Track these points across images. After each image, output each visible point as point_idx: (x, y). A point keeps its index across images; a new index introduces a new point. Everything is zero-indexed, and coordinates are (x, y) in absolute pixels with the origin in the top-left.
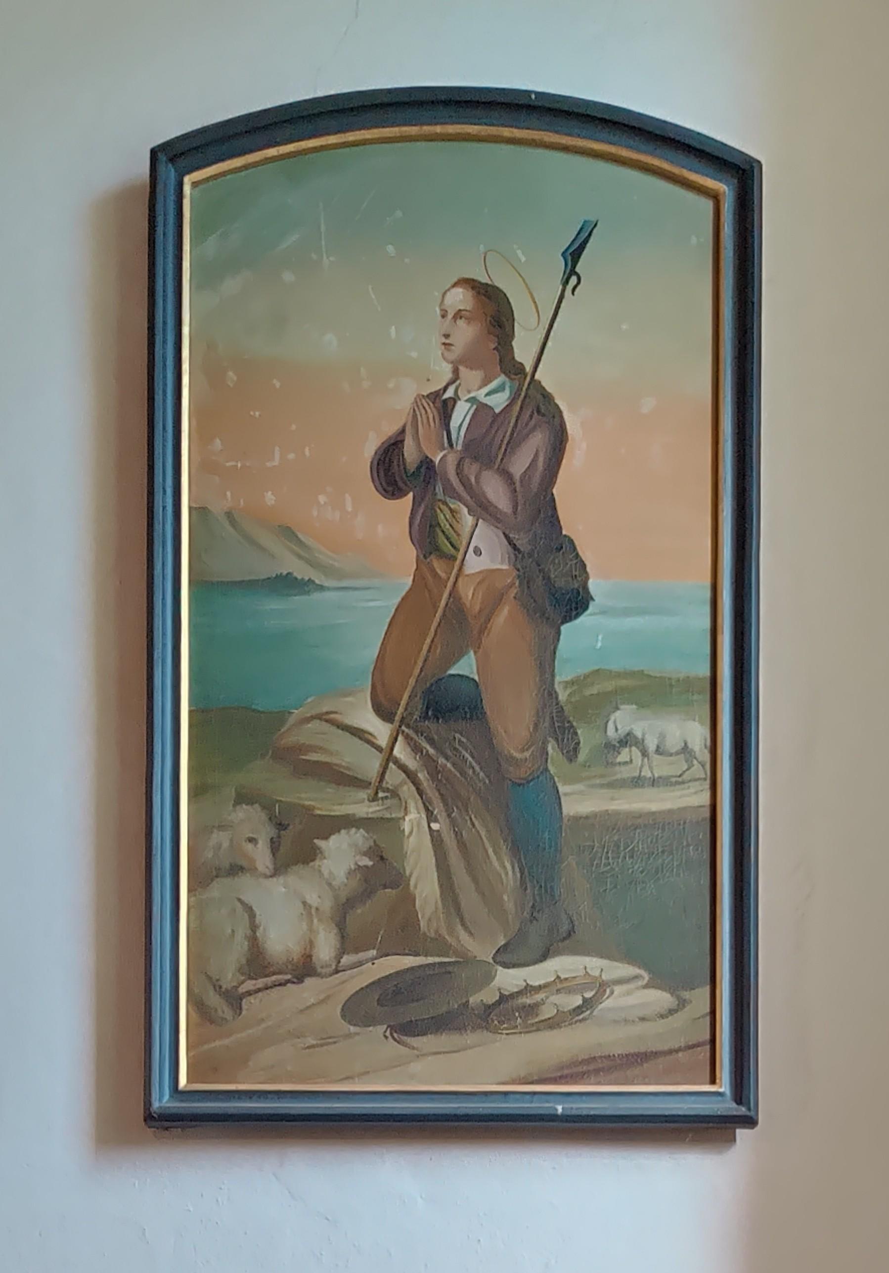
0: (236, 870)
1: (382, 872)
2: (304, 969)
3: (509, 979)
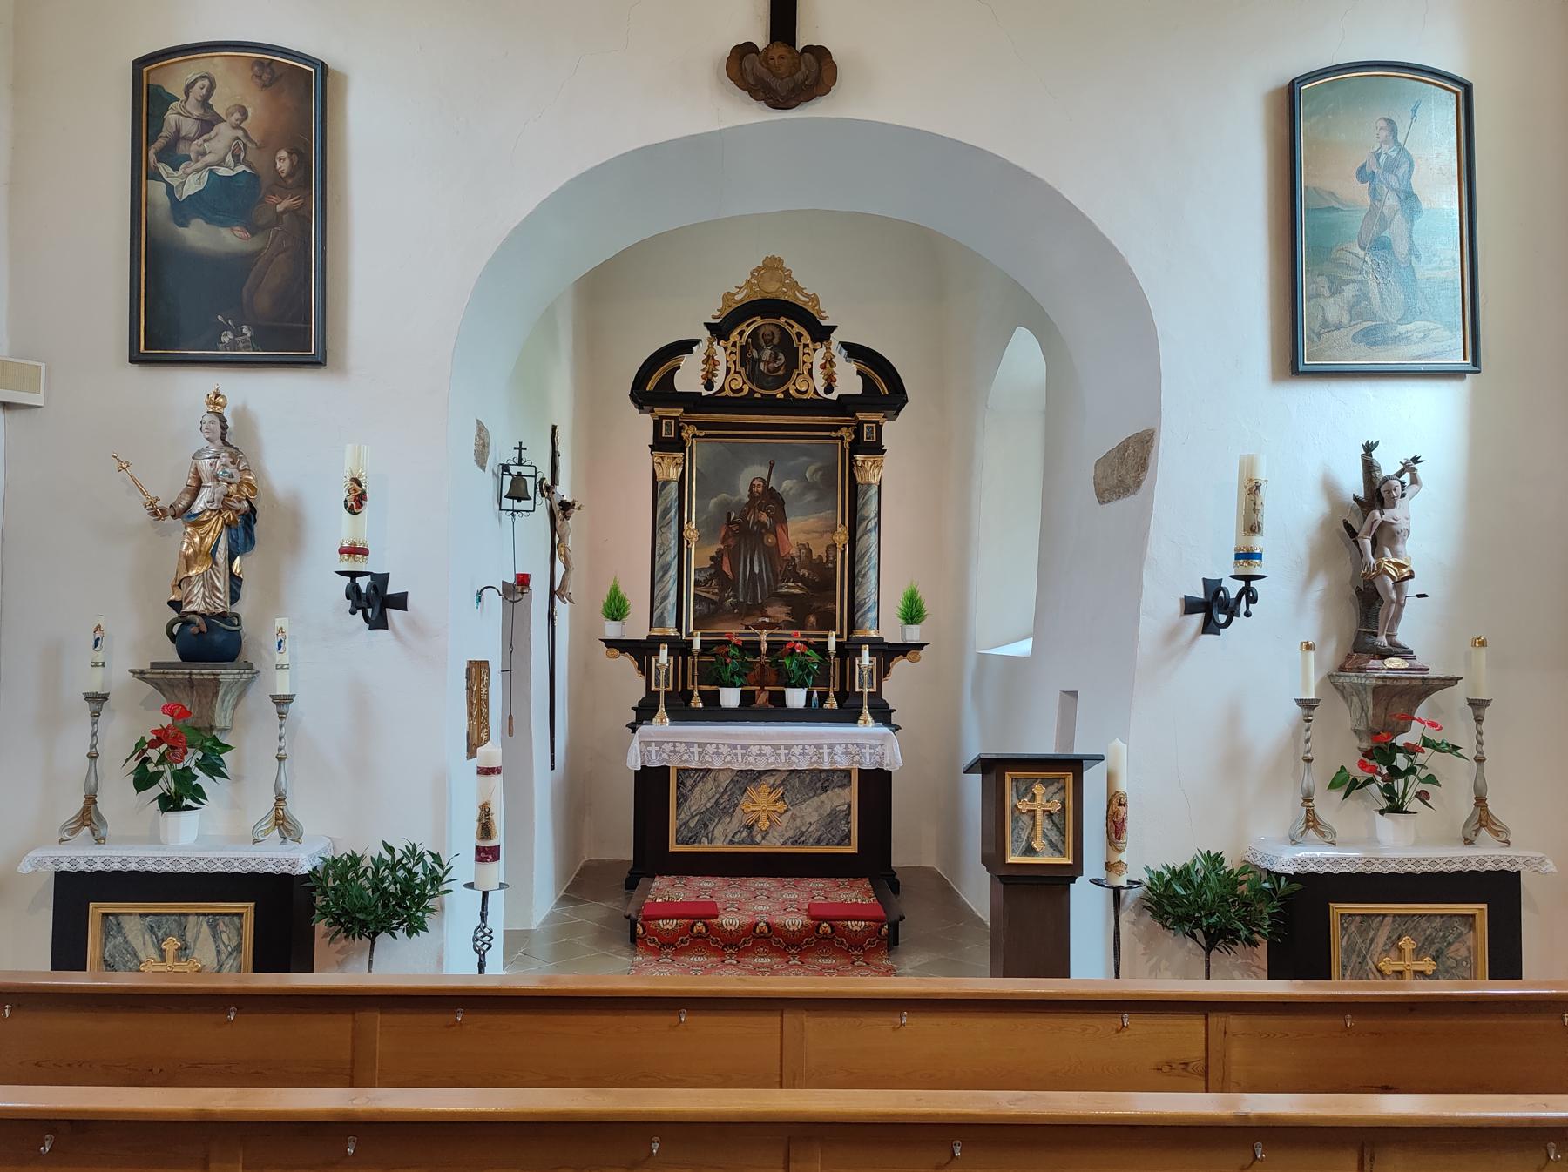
0: (1318, 296)
1: (1364, 296)
2: (1339, 327)
3: (1401, 329)
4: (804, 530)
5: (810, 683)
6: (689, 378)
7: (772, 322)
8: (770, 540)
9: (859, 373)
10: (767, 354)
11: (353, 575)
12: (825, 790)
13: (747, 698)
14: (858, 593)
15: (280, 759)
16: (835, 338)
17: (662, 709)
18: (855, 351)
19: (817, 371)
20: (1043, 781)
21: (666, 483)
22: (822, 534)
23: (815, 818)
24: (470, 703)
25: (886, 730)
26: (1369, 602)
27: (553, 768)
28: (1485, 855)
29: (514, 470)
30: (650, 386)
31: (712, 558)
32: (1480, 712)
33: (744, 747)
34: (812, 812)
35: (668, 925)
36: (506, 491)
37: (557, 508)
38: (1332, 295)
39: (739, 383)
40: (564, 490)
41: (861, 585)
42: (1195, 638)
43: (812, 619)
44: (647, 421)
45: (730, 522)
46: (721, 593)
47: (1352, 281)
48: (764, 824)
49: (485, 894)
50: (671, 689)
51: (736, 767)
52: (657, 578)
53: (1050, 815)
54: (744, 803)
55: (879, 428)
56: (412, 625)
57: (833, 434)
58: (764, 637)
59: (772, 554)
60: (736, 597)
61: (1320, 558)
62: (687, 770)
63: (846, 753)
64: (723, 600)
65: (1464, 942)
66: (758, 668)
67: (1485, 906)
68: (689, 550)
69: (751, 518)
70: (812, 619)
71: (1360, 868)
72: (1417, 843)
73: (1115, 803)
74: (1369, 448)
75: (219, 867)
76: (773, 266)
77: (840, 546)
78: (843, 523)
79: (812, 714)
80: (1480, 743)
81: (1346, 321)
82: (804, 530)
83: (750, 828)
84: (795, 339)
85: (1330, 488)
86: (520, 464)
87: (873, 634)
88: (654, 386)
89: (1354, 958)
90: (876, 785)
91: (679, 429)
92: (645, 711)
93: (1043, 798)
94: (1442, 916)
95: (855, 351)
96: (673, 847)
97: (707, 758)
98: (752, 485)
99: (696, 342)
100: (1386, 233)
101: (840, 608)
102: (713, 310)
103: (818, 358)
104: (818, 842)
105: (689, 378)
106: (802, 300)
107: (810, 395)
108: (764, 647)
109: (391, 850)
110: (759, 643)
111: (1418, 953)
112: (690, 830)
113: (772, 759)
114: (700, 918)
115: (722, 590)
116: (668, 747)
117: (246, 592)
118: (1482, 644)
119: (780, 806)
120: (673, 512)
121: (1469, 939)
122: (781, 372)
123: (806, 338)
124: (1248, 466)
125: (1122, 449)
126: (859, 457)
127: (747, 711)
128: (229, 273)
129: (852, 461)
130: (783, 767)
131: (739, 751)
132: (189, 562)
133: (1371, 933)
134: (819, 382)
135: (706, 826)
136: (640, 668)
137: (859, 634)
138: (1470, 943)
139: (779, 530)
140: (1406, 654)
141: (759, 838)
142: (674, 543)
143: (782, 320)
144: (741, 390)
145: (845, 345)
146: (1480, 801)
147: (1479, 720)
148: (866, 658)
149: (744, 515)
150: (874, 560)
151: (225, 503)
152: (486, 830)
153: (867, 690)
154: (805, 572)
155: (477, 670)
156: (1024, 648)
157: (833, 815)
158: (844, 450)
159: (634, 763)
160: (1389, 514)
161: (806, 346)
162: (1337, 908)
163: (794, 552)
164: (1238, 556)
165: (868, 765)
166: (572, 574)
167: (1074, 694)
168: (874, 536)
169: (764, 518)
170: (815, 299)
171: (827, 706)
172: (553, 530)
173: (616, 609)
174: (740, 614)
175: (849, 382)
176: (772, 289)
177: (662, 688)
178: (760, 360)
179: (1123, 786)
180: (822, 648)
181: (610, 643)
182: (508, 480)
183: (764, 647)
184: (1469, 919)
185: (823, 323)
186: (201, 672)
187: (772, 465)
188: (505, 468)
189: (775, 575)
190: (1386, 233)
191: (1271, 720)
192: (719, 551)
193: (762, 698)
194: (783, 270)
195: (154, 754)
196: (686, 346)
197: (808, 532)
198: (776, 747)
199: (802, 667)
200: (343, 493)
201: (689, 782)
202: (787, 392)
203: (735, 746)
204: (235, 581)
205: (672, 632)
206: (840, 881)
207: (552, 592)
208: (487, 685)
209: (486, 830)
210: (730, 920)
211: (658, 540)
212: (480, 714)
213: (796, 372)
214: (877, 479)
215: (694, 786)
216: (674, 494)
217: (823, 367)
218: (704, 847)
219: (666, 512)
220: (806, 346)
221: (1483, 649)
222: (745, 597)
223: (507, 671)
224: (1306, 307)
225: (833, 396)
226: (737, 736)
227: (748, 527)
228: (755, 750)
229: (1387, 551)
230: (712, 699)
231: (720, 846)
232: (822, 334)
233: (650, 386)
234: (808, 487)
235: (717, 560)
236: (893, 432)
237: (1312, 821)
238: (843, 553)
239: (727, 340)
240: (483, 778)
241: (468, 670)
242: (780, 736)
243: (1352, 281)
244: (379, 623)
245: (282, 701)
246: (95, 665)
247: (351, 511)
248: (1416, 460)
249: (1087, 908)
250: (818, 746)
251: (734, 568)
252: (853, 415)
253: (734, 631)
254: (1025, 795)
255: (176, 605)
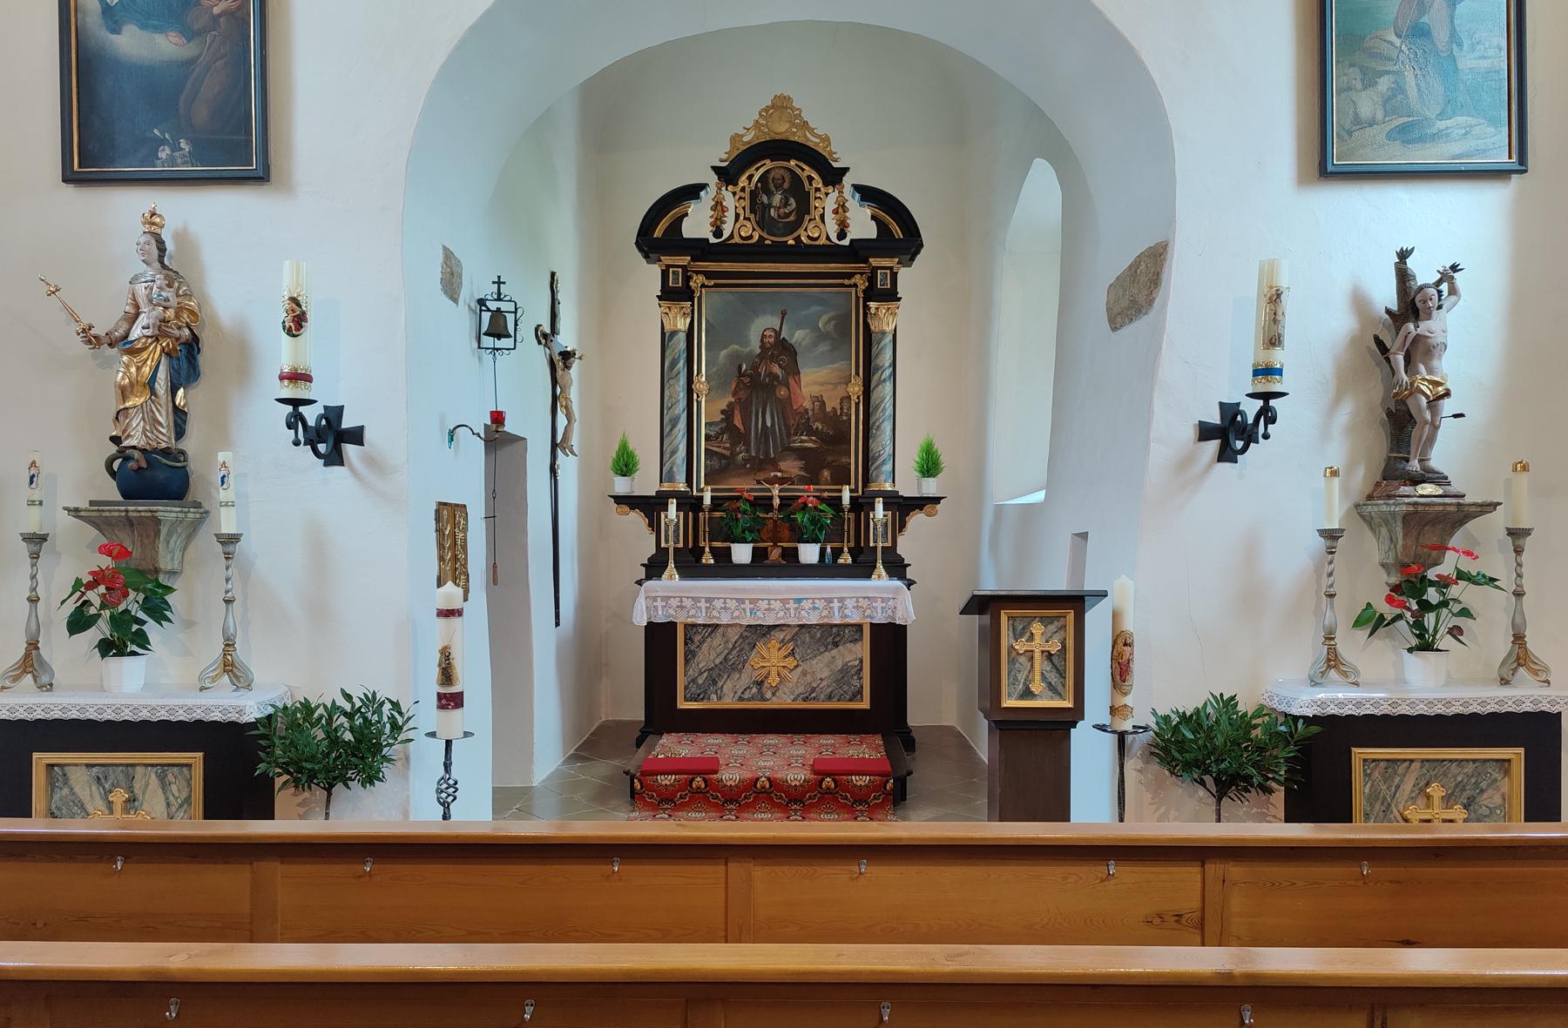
0: (1349, 89)
1: (1398, 89)
2: (1372, 123)
3: (1441, 125)
4: (818, 381)
5: (822, 538)
6: (697, 223)
7: (781, 163)
8: (783, 392)
9: (873, 218)
10: (777, 199)
11: (296, 403)
12: (836, 645)
13: (759, 555)
14: (873, 445)
15: (228, 602)
16: (848, 180)
17: (671, 565)
18: (868, 194)
19: (829, 216)
20: (1042, 619)
21: (674, 333)
22: (836, 385)
23: (826, 673)
24: (441, 546)
25: (898, 583)
26: (1402, 424)
27: (557, 624)
28: (1523, 696)
29: (493, 306)
30: (658, 233)
31: (723, 412)
32: (1520, 542)
33: (752, 601)
34: (822, 666)
35: (666, 780)
36: (485, 328)
37: (557, 358)
38: (1365, 88)
39: (749, 231)
40: (567, 338)
41: (875, 436)
42: (1210, 466)
43: (826, 473)
44: (655, 271)
45: (741, 375)
46: (733, 445)
47: (1388, 72)
48: (774, 680)
49: (448, 743)
50: (681, 545)
51: (745, 623)
52: (666, 430)
53: (1049, 656)
54: (754, 659)
55: (894, 276)
56: (372, 462)
57: (846, 282)
58: (776, 492)
59: (784, 407)
60: (748, 451)
61: (1346, 379)
62: (694, 626)
63: (857, 607)
64: (734, 455)
65: (1498, 789)
66: (770, 524)
67: (1521, 750)
68: (699, 403)
69: (762, 370)
70: (826, 473)
71: (1385, 709)
72: (1449, 683)
73: (1121, 645)
74: (1403, 255)
75: (163, 715)
76: (781, 105)
77: (854, 398)
78: (857, 373)
79: (825, 569)
80: (1519, 576)
81: (1380, 116)
82: (818, 381)
83: (760, 684)
84: (806, 183)
85: (1359, 303)
86: (499, 299)
87: (888, 487)
88: (658, 235)
89: (1378, 805)
90: (889, 642)
91: (687, 279)
92: (654, 568)
93: (1041, 637)
94: (1474, 761)
95: (868, 194)
96: (682, 705)
97: (715, 613)
98: (763, 336)
99: (703, 187)
100: (1425, 19)
101: (854, 462)
102: (720, 153)
103: (830, 203)
104: (830, 698)
105: (697, 223)
106: (812, 141)
107: (823, 241)
108: (776, 502)
109: (348, 697)
110: (771, 498)
111: (1448, 801)
112: (699, 687)
113: (781, 614)
114: (698, 773)
115: (733, 445)
116: (674, 602)
117: (193, 427)
118: (1525, 468)
119: (791, 662)
120: (682, 364)
121: (1504, 785)
122: (792, 218)
123: (818, 182)
124: (1268, 270)
125: (1134, 267)
126: (872, 305)
127: (760, 567)
128: (164, 90)
129: (866, 308)
130: (793, 621)
131: (747, 605)
132: (124, 393)
133: (1397, 780)
134: (832, 228)
135: (715, 682)
136: (651, 525)
137: (873, 487)
138: (1505, 789)
139: (792, 382)
140: (1439, 479)
141: (768, 695)
142: (682, 395)
143: (793, 163)
144: (751, 237)
145: (857, 188)
146: (1519, 638)
147: (1518, 551)
148: (879, 511)
149: (755, 367)
150: (889, 411)
151: (161, 331)
152: (447, 675)
153: (880, 545)
154: (818, 425)
155: (449, 517)
156: (1039, 496)
157: (845, 671)
158: (857, 298)
159: (641, 619)
160: (1424, 327)
161: (818, 190)
162: (1359, 754)
163: (807, 404)
164: (1256, 373)
165: (880, 618)
166: (576, 426)
167: (1084, 536)
168: (888, 386)
169: (776, 370)
170: (826, 139)
171: (841, 561)
172: (554, 382)
173: (625, 465)
174: (752, 469)
175: (863, 225)
176: (781, 129)
177: (671, 543)
178: (770, 206)
179: (1129, 625)
180: (835, 503)
181: (619, 500)
182: (486, 316)
183: (776, 502)
184: (1504, 763)
185: (835, 165)
186: (139, 509)
187: (784, 314)
188: (481, 302)
189: (788, 427)
190: (1425, 19)
191: (1292, 554)
192: (730, 405)
193: (775, 554)
194: (793, 109)
195: (94, 596)
196: (692, 192)
197: (822, 384)
198: (784, 601)
199: (813, 521)
200: (281, 315)
201: (697, 638)
202: (798, 239)
203: (741, 601)
204: (180, 415)
205: (682, 487)
206: (851, 738)
207: (554, 445)
208: (465, 530)
209: (447, 675)
210: (730, 776)
211: (667, 393)
212: (455, 558)
213: (807, 218)
214: (892, 327)
215: (702, 642)
216: (683, 345)
217: (836, 212)
218: (713, 704)
219: (674, 363)
220: (818, 190)
221: (1525, 474)
222: (757, 452)
223: (490, 517)
224: (1335, 101)
225: (846, 242)
226: (745, 590)
227: (760, 378)
228: (764, 605)
229: (1422, 368)
230: (723, 556)
231: (729, 702)
232: (834, 176)
233: (658, 233)
234: (822, 337)
235: (728, 414)
236: (907, 278)
237: (1333, 660)
238: (857, 404)
239: (736, 184)
240: (442, 621)
241: (437, 511)
242: (788, 590)
243: (1388, 72)
244: (334, 459)
245: (230, 540)
246: (32, 503)
247: (289, 332)
248: (1454, 268)
249: (1089, 755)
250: (830, 601)
251: (746, 421)
252: (866, 261)
253: (744, 485)
254: (1021, 635)
255: (115, 440)
